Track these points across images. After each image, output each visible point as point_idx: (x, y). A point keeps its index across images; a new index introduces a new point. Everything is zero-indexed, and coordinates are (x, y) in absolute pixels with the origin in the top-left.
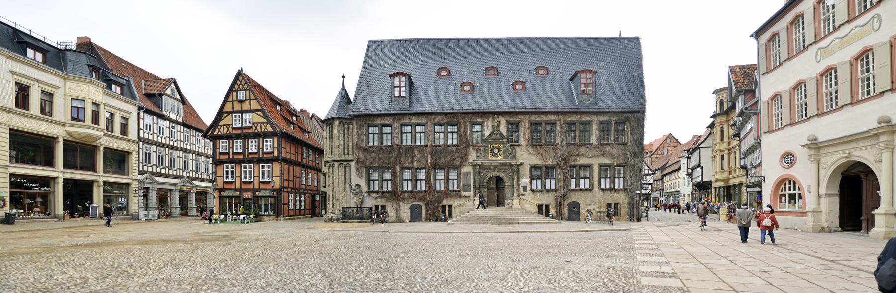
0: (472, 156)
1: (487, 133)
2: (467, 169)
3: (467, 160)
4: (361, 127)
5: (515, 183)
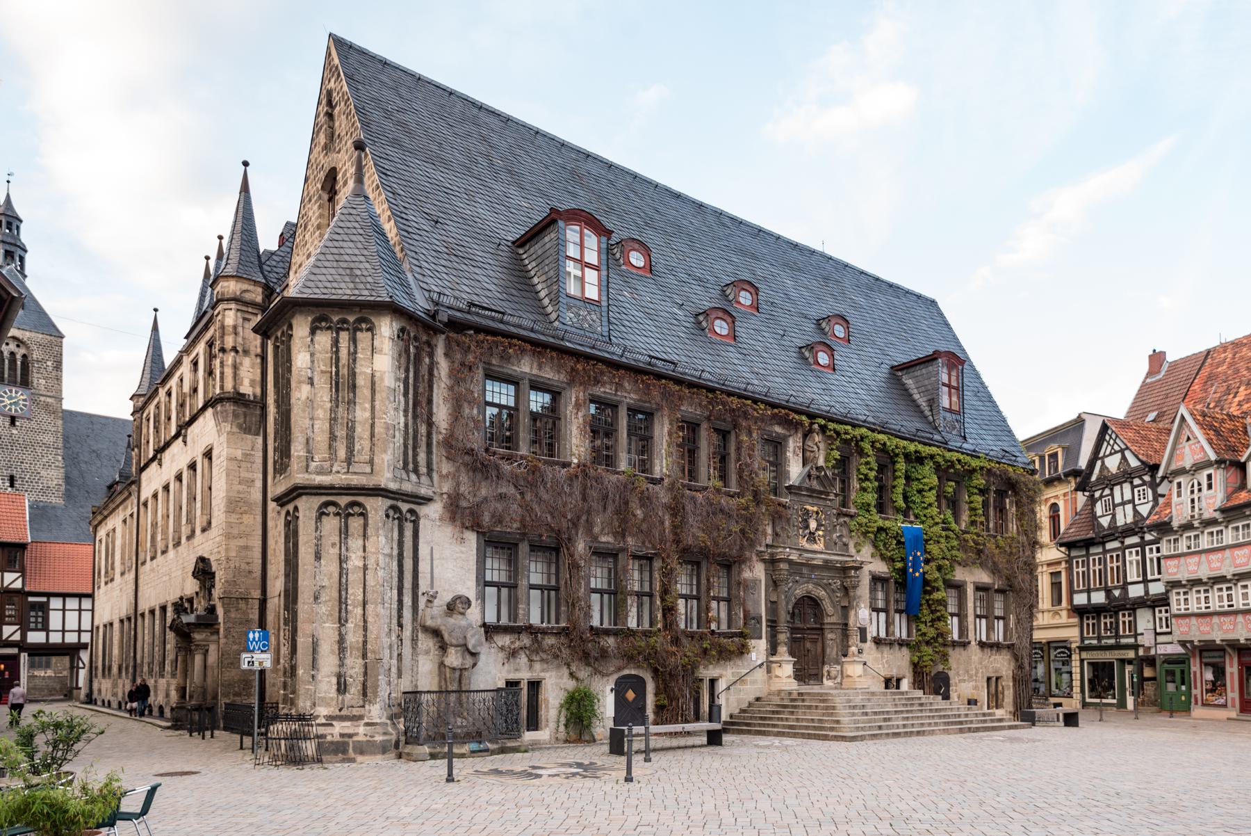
2: (757, 572)
3: (752, 544)
4: (460, 373)
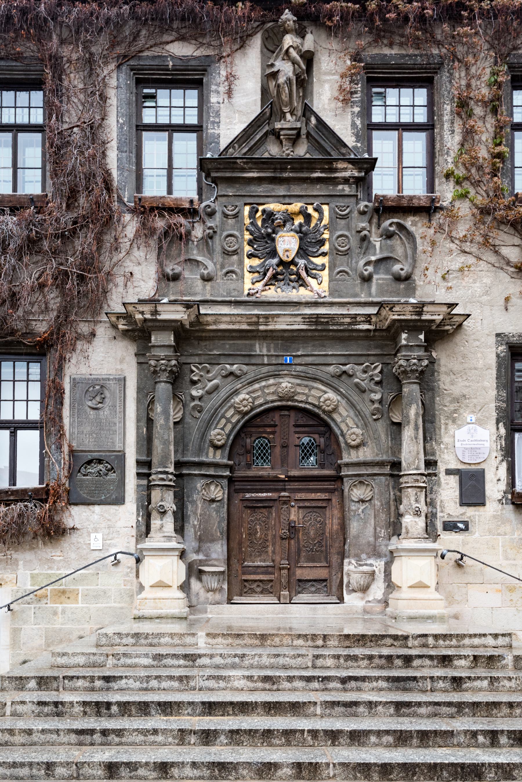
0: (136, 277)
1: (229, 128)
2: (104, 357)
3: (95, 303)
5: (411, 452)
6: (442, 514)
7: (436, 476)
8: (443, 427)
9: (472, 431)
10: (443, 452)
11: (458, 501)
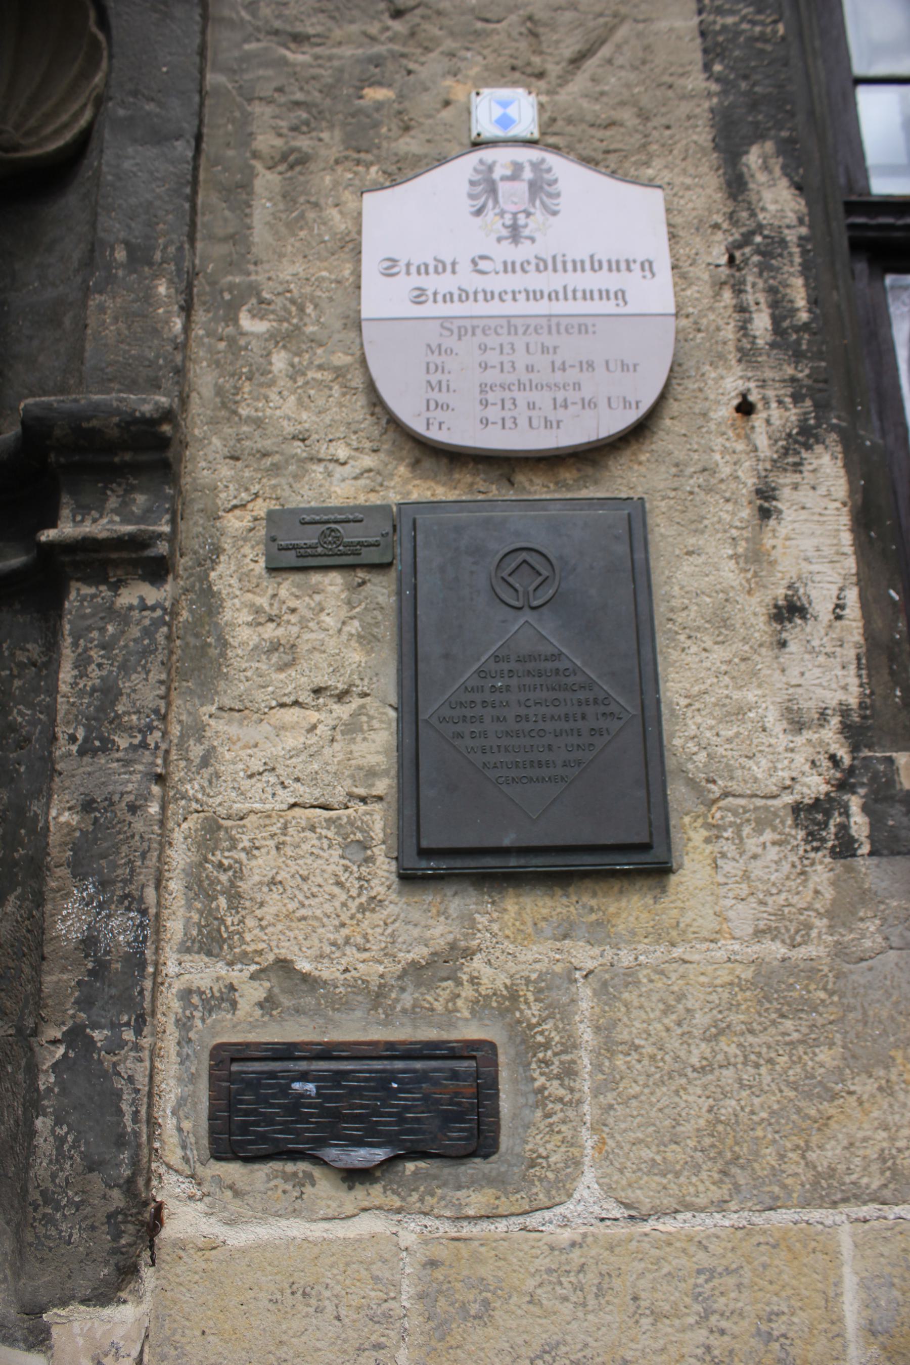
6: (205, 973)
7: (158, 570)
8: (267, 181)
9: (513, 195)
10: (260, 374)
11: (378, 822)
